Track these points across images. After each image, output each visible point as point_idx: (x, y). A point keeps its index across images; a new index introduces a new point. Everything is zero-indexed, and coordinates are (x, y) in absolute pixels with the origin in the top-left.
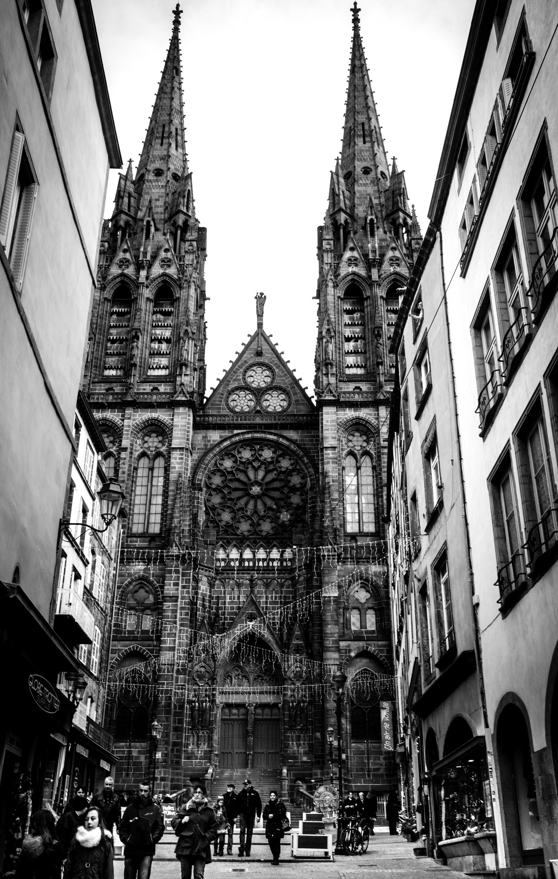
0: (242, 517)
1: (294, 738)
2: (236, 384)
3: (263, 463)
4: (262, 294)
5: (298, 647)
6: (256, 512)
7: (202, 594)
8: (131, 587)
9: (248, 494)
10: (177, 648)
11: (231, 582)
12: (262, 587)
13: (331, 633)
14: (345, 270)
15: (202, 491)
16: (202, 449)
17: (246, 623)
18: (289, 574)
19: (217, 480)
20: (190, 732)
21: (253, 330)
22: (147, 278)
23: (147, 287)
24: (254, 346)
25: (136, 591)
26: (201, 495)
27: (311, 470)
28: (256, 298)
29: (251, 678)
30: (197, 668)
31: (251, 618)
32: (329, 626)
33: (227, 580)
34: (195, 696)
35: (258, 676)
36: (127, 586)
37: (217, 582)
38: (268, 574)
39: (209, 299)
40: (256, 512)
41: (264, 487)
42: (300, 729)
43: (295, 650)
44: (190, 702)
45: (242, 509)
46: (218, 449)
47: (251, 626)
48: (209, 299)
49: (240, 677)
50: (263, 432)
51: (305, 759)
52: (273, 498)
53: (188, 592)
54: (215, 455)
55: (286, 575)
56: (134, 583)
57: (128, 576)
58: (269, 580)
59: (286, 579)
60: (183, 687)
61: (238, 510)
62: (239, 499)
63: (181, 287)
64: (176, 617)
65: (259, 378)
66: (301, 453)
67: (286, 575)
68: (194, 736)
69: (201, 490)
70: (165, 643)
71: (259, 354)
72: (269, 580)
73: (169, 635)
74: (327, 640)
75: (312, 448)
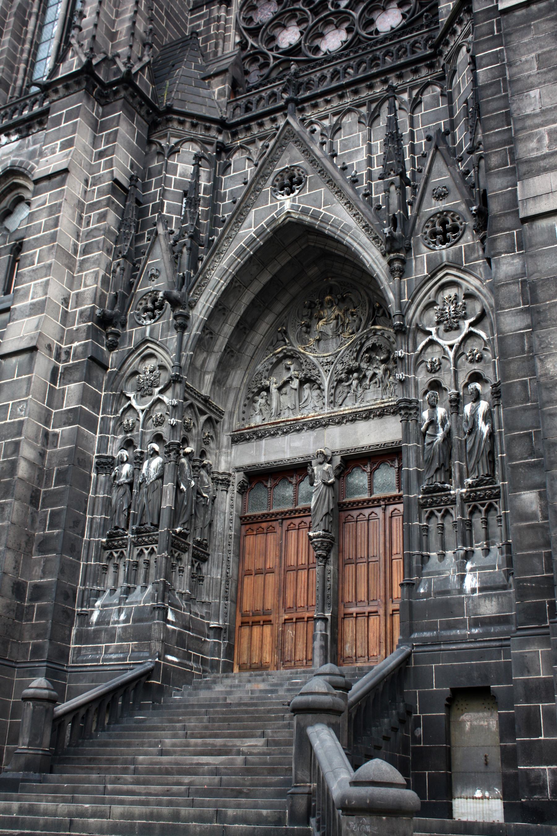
0: (327, 22)
1: (451, 536)
5: (444, 223)
7: (178, 184)
12: (357, 127)
17: (274, 198)
18: (431, 66)
20: (107, 553)
26: (228, 12)
30: (134, 362)
31: (290, 182)
32: (534, 93)
33: (261, 144)
34: (128, 444)
35: (350, 372)
37: (237, 156)
38: (371, 87)
42: (465, 500)
43: (434, 234)
44: (107, 464)
49: (295, 384)
51: (489, 608)
55: (424, 72)
58: (374, 106)
59: (427, 85)
60: (74, 416)
67: (424, 72)
68: (117, 567)
72: (374, 106)
74: (530, 137)
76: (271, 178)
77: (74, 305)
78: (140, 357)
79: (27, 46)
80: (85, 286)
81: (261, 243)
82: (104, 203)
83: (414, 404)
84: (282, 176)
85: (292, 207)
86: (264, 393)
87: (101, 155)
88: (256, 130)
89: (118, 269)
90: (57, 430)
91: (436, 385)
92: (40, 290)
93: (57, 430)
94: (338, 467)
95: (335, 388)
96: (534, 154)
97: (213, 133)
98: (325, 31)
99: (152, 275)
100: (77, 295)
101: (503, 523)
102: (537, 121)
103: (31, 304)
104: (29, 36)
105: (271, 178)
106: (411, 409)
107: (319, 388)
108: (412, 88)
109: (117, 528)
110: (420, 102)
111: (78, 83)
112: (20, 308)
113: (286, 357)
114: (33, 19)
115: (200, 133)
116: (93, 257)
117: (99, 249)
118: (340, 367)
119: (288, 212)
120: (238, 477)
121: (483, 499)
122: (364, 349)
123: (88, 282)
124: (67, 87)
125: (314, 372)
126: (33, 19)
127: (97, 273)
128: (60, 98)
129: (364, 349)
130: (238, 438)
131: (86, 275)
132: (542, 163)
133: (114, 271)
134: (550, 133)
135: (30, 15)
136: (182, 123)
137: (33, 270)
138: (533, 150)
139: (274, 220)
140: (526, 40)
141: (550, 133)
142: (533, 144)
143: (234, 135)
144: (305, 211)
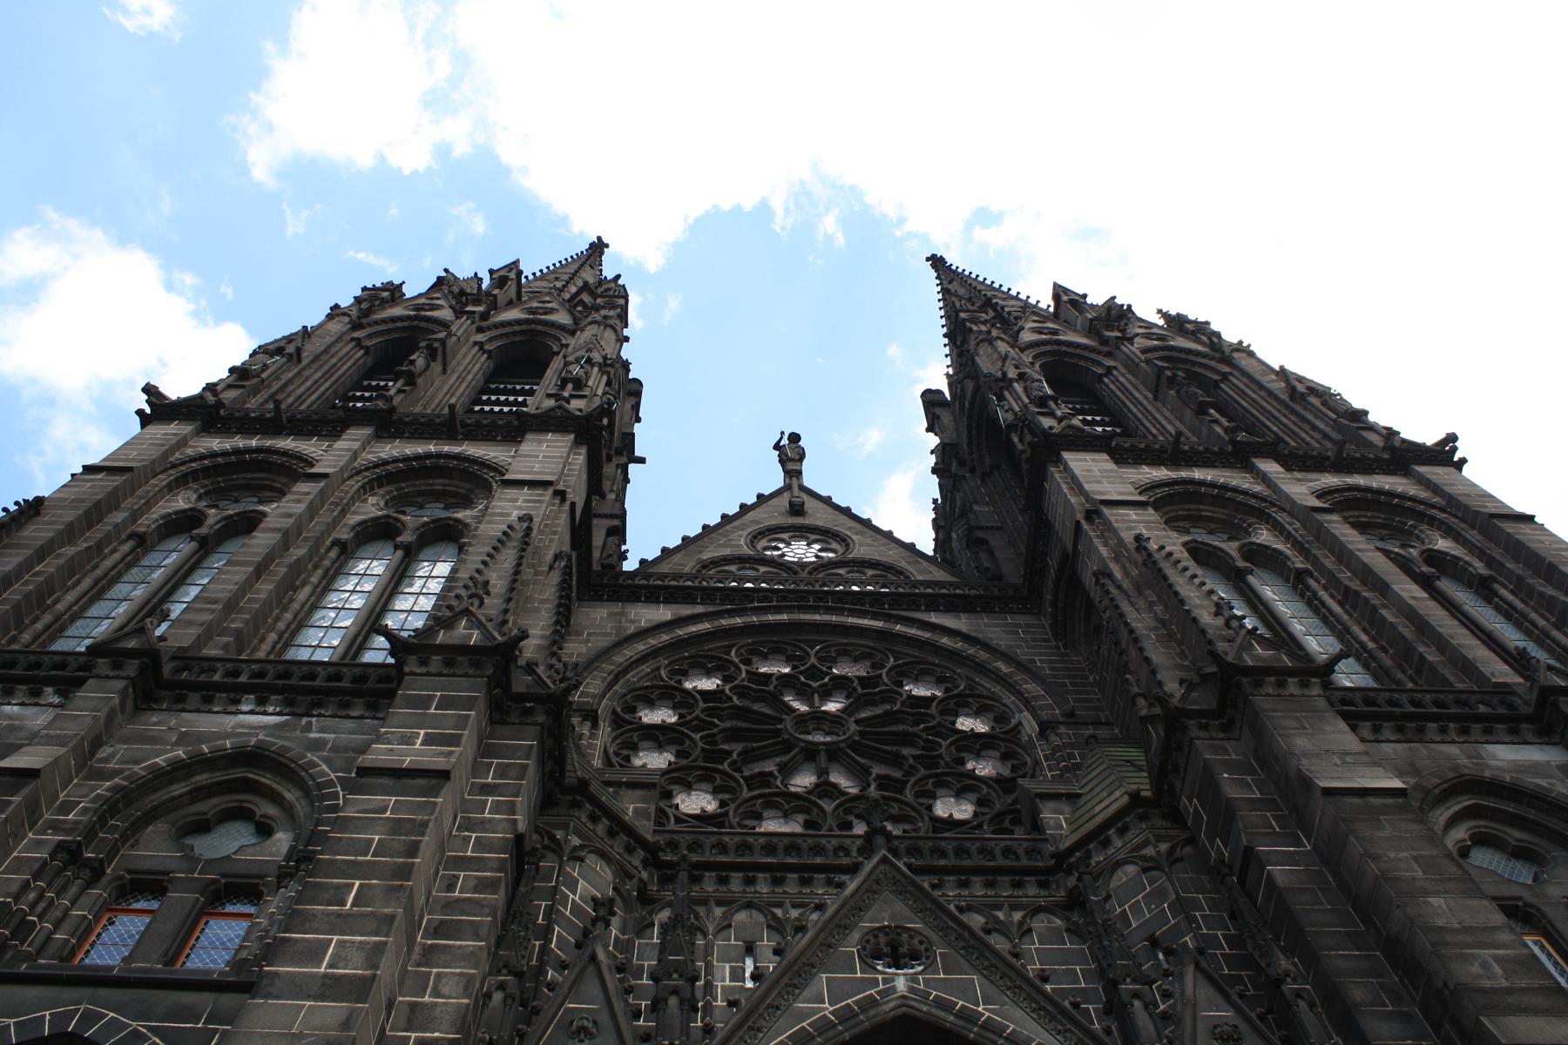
2: (727, 552)
3: (841, 684)
4: (795, 438)
6: (825, 789)
8: (179, 789)
9: (788, 746)
10: (380, 993)
11: (741, 916)
13: (1466, 930)
14: (1027, 337)
15: (595, 725)
16: (610, 634)
18: (1043, 885)
19: (661, 715)
21: (774, 479)
22: (484, 316)
23: (480, 330)
24: (784, 501)
25: (202, 826)
27: (1031, 688)
28: (777, 447)
33: (718, 911)
36: (162, 777)
39: (642, 460)
40: (825, 789)
41: (853, 727)
45: (765, 779)
46: (665, 637)
47: (901, 984)
48: (642, 460)
50: (829, 610)
52: (895, 760)
53: (511, 808)
54: (655, 653)
55: (1032, 890)
56: (202, 778)
57: (178, 743)
61: (751, 781)
62: (748, 757)
63: (573, 333)
64: (413, 849)
65: (800, 552)
66: (983, 655)
69: (591, 716)
70: (314, 953)
71: (796, 509)
73: (343, 923)
75: (1019, 647)
76: (856, 936)
77: (402, 1021)
79: (289, 616)
80: (436, 994)
81: (847, 1036)
82: (495, 864)
84: (876, 937)
85: (911, 990)
87: (487, 789)
88: (709, 885)
89: (498, 997)
92: (357, 957)
96: (1487, 983)
97: (637, 863)
98: (765, 814)
99: (583, 1029)
100: (413, 1007)
102: (1461, 938)
103: (326, 976)
104: (296, 606)
105: (856, 936)
108: (1014, 907)
110: (1030, 930)
111: (476, 665)
112: (292, 975)
114: (307, 590)
115: (617, 847)
116: (460, 947)
117: (478, 938)
119: (904, 997)
123: (445, 990)
124: (449, 663)
126: (307, 590)
127: (470, 980)
128: (428, 674)
131: (439, 975)
132: (1511, 999)
133: (488, 996)
134: (1499, 960)
135: (304, 584)
136: (594, 819)
137: (339, 915)
138: (1481, 976)
139: (871, 1002)
140: (1382, 834)
141: (1497, 959)
142: (1475, 968)
143: (666, 880)
144: (939, 1002)
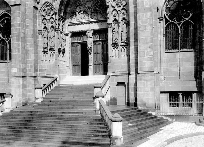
29: (89, 12)
44: (40, 32)
78: (45, 6)
83: (111, 24)
86: (75, 14)
90: (28, 24)
91: (115, 20)
93: (28, 24)
94: (93, 33)
95: (91, 14)
101: (128, 51)
106: (110, 25)
107: (88, 14)
109: (45, 47)
113: (79, 5)
118: (92, 9)
120: (70, 34)
121: (124, 46)
122: (98, 5)
125: (87, 10)
129: (98, 5)
130: (70, 25)
